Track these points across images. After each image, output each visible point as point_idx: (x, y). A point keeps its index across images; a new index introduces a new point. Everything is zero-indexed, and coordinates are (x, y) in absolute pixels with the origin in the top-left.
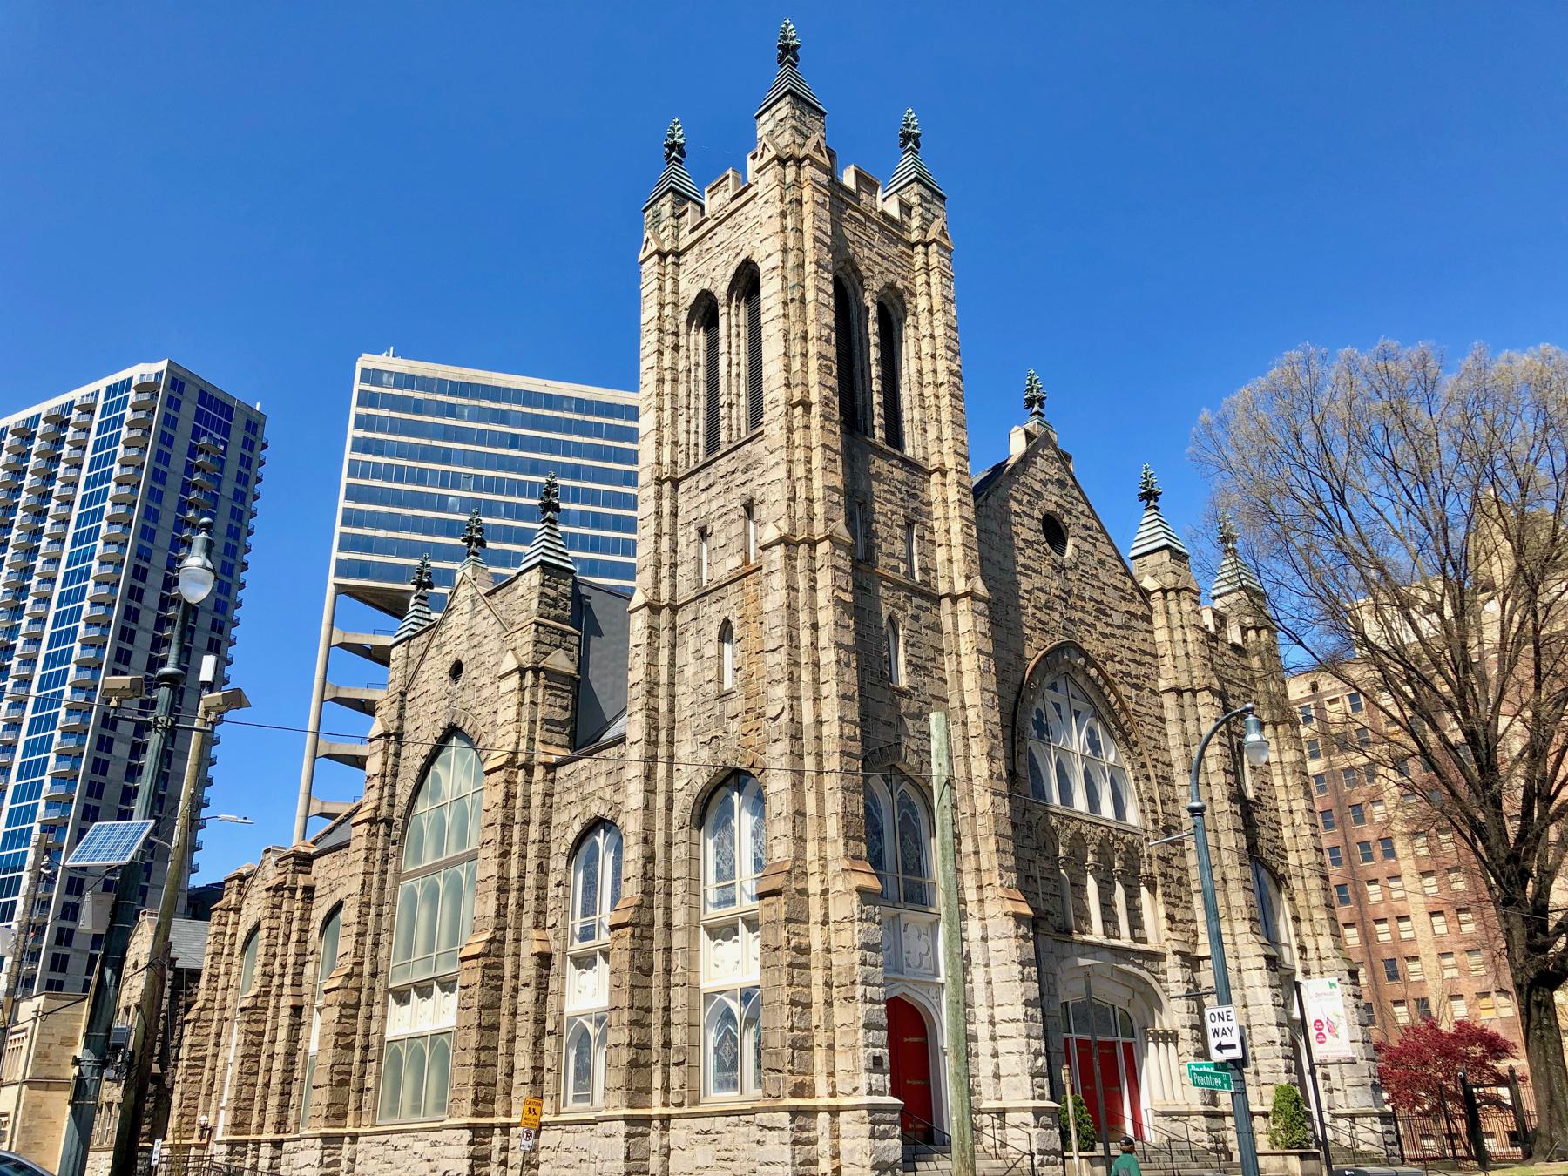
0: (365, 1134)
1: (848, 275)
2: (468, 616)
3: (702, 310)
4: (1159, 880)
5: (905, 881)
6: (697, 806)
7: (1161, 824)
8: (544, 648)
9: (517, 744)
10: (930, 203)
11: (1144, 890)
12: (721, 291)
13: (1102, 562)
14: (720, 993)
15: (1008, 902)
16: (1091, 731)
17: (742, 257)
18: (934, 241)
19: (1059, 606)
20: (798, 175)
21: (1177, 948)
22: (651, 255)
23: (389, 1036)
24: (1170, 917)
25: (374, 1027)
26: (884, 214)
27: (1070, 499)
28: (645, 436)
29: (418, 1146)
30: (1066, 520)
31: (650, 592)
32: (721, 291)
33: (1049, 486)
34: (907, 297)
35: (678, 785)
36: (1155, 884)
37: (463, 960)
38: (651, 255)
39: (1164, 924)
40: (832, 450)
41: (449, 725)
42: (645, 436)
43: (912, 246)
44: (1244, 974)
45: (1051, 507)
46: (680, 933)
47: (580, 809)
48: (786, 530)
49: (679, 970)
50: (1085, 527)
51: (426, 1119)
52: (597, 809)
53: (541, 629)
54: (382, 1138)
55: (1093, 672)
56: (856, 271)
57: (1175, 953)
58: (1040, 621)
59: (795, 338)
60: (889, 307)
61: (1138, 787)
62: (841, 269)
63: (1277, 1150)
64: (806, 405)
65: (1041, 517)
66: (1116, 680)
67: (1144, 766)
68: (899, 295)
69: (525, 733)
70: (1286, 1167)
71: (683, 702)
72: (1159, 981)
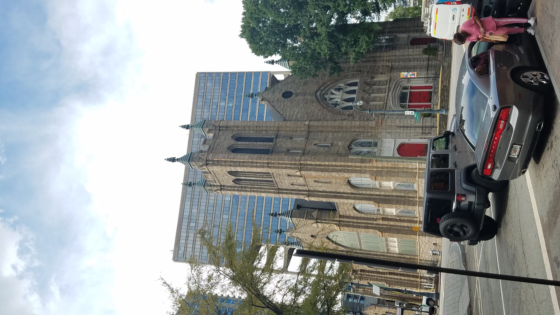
0: (420, 258)
1: (231, 148)
2: (300, 233)
3: (236, 182)
4: (373, 75)
5: (373, 147)
6: (354, 188)
7: (359, 73)
8: (312, 217)
9: (334, 224)
10: (208, 125)
11: (375, 80)
12: (234, 178)
13: (293, 81)
14: (394, 186)
15: (378, 125)
16: (336, 89)
17: (227, 173)
18: (219, 125)
19: (306, 97)
20: (211, 160)
21: (389, 73)
22: (221, 192)
23: (398, 252)
24: (382, 74)
25: (396, 256)
26: (213, 138)
27: (278, 90)
28: (267, 195)
29: (423, 246)
30: (284, 91)
31: (305, 196)
32: (234, 178)
33: (275, 95)
34: (234, 133)
35: (349, 192)
36: (373, 76)
37: (382, 236)
38: (221, 192)
39: (383, 75)
40: (279, 159)
41: (326, 238)
42: (267, 195)
43: (220, 130)
44: (396, 55)
45: (281, 94)
46: (381, 193)
47: (351, 211)
48: (297, 170)
49: (389, 194)
50: (284, 85)
51: (417, 245)
52: (351, 207)
53: (307, 218)
54: (421, 254)
55: (322, 88)
56: (230, 147)
57: (390, 74)
58: (311, 103)
59: (252, 164)
60: (237, 137)
61: (350, 78)
62: (230, 150)
63: (437, 55)
64: (268, 163)
65: (284, 99)
66: (323, 81)
67: (344, 76)
68: (234, 135)
69: (332, 222)
70: (440, 55)
71: (331, 190)
72: (397, 79)
